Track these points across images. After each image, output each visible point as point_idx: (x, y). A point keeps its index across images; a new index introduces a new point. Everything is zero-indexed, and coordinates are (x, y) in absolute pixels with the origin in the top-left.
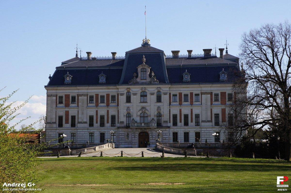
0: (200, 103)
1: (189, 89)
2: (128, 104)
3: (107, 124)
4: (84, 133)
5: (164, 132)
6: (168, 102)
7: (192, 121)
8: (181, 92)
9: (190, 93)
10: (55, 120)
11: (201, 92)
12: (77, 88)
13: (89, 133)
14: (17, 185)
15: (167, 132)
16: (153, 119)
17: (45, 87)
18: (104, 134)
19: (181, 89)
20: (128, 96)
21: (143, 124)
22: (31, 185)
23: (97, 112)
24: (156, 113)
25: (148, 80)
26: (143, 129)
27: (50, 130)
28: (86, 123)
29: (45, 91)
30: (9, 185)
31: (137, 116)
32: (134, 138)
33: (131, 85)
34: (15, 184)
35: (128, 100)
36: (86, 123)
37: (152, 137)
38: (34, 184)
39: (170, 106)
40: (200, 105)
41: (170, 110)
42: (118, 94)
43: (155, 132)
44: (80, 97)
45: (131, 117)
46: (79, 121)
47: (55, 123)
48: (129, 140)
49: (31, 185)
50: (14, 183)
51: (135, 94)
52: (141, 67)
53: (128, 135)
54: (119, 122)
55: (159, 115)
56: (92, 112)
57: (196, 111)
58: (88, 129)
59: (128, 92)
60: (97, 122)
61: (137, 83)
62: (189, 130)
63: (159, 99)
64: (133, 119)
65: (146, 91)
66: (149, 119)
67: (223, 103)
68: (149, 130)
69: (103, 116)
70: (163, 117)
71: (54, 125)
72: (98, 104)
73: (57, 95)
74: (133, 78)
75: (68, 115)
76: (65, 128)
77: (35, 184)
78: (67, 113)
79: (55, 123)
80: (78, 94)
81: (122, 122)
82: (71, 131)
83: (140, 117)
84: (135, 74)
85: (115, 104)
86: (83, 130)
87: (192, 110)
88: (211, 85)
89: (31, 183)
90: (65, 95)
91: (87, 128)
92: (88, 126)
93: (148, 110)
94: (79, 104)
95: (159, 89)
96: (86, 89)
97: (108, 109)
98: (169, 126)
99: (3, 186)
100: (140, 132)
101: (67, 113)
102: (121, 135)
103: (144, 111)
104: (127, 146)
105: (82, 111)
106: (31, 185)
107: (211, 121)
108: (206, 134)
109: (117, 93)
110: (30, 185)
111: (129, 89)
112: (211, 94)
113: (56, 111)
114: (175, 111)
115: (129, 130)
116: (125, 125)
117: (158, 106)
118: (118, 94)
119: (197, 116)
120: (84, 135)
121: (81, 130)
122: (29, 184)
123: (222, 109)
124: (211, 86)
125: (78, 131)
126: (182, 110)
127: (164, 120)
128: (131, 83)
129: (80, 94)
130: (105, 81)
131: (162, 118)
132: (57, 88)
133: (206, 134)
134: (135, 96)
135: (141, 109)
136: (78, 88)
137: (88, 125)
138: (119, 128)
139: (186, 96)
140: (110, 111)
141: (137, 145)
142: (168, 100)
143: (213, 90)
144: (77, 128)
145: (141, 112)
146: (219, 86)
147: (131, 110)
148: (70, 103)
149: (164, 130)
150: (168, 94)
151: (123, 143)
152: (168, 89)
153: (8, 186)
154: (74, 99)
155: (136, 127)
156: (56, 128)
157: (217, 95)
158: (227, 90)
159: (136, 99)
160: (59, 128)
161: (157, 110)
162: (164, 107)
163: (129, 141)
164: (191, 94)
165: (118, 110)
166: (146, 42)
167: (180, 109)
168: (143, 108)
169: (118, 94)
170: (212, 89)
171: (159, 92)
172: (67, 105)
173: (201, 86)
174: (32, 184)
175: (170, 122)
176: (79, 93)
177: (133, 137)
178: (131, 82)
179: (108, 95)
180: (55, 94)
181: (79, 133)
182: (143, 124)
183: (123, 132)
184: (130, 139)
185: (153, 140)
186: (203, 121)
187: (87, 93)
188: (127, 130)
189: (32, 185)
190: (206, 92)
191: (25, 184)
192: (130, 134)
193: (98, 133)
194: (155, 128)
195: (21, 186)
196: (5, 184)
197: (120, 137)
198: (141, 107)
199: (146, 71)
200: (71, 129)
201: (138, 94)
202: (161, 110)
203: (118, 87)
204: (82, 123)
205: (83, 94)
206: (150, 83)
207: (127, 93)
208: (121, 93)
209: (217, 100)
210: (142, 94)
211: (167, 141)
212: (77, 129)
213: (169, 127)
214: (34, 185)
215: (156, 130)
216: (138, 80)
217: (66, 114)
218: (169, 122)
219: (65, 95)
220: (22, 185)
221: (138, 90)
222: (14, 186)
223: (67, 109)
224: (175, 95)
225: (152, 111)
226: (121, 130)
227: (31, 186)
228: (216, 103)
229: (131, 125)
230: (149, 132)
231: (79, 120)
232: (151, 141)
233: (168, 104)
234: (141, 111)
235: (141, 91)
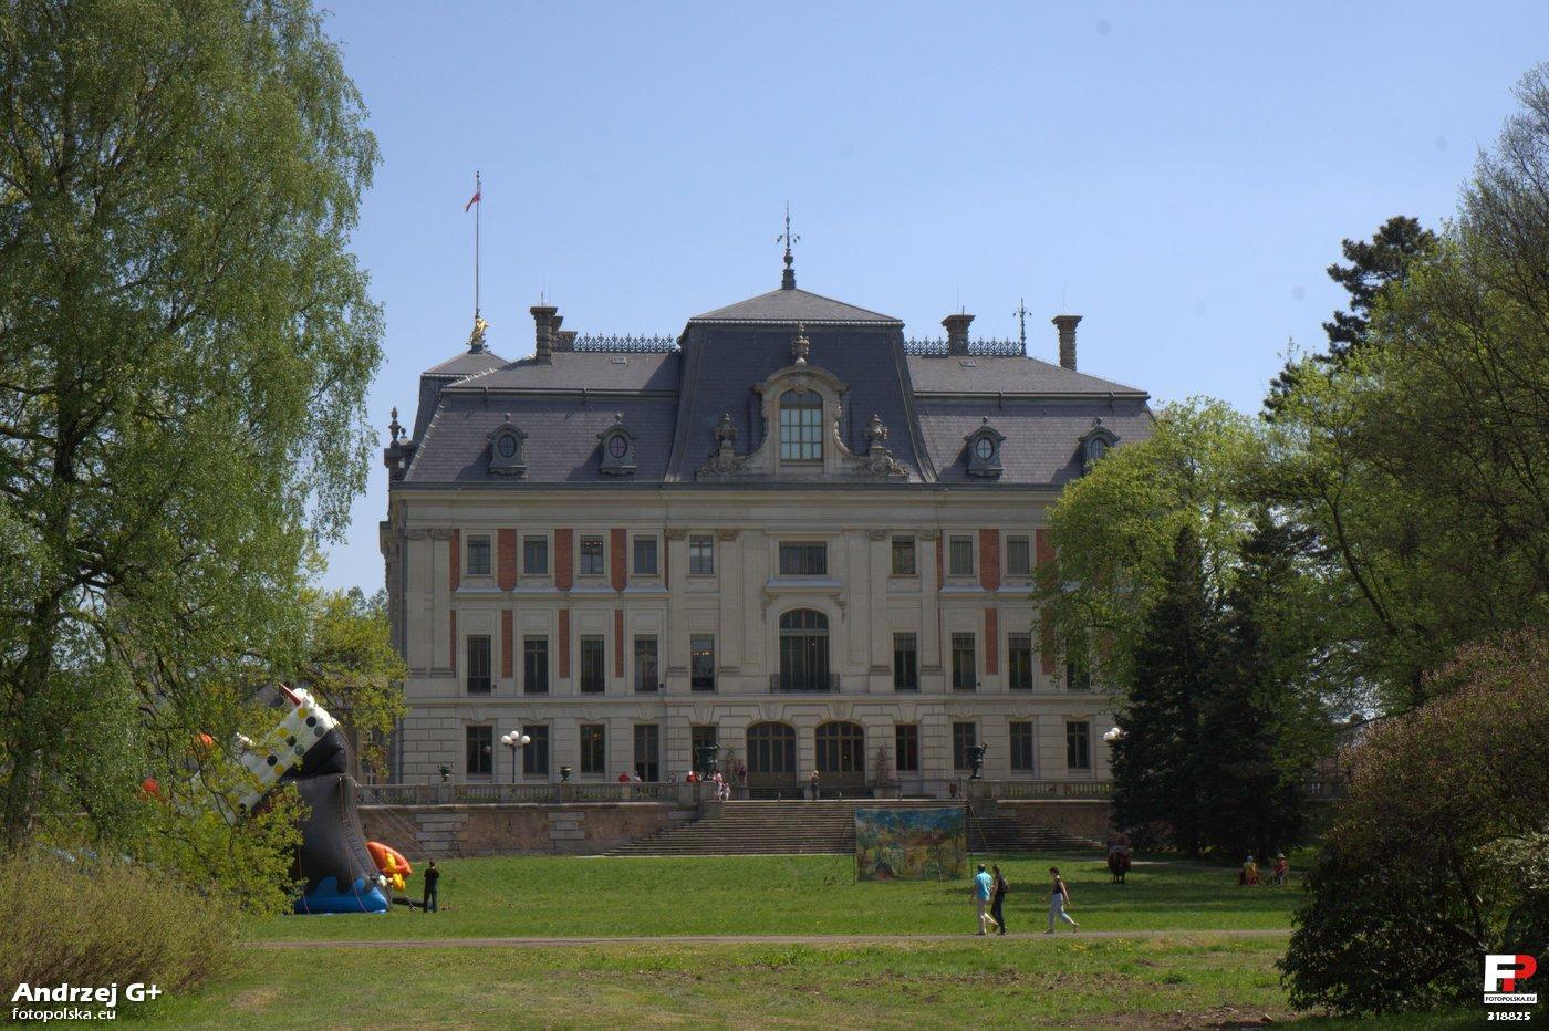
14: (78, 995)
22: (141, 994)
30: (42, 995)
34: (69, 992)
38: (154, 992)
49: (141, 994)
50: (65, 986)
69: (597, 642)
77: (159, 992)
89: (142, 986)
99: (15, 999)
106: (141, 994)
110: (138, 993)
122: (134, 994)
140: (629, 616)
153: (37, 999)
174: (148, 992)
189: (147, 997)
191: (114, 991)
195: (94, 999)
196: (23, 990)
214: (157, 995)
220: (98, 996)
222: (64, 998)
227: (141, 998)
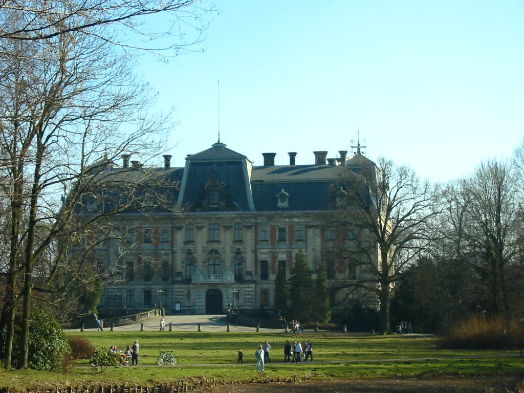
5: (247, 289)
13: (127, 291)
15: (251, 289)
18: (150, 292)
21: (212, 277)
32: (199, 298)
37: (228, 298)
81: (180, 274)
115: (191, 286)
149: (247, 286)
182: (212, 277)
183: (181, 290)
188: (187, 286)
192: (192, 292)
194: (232, 284)
226: (177, 286)
230: (223, 290)
233: (254, 245)
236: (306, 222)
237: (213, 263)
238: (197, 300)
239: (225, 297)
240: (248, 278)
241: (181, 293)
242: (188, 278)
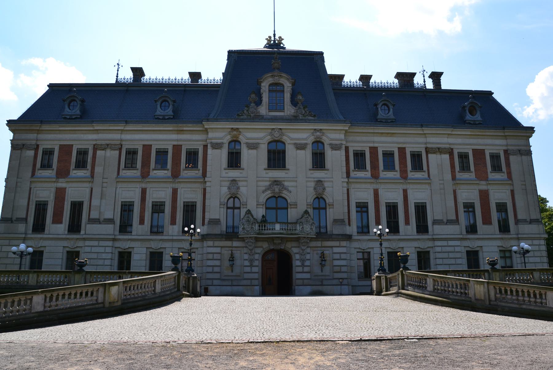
0: (426, 176)
1: (395, 139)
2: (234, 174)
3: (171, 227)
4: (102, 250)
5: (336, 250)
6: (344, 169)
7: (407, 222)
8: (376, 145)
9: (399, 148)
10: (25, 212)
11: (426, 148)
12: (93, 126)
15: (344, 250)
16: (306, 212)
17: (10, 123)
19: (376, 139)
20: (234, 151)
23: (144, 192)
24: (310, 200)
25: (289, 110)
26: (275, 241)
27: (8, 241)
28: (110, 221)
29: (10, 135)
31: (257, 205)
32: (251, 266)
33: (242, 120)
35: (234, 161)
36: (110, 221)
37: (303, 266)
39: (350, 180)
40: (426, 179)
41: (348, 190)
42: (207, 146)
43: (308, 250)
44: (99, 153)
45: (239, 208)
46: (91, 217)
47: (25, 220)
48: (234, 274)
51: (253, 146)
52: (270, 80)
53: (232, 259)
54: (206, 221)
55: (320, 203)
56: (132, 194)
57: (417, 195)
58: (114, 240)
59: (235, 141)
60: (142, 222)
61: (259, 118)
62: (401, 244)
63: (319, 161)
64: (249, 212)
65: (285, 139)
66: (293, 214)
67: (482, 176)
68: (294, 244)
70: (331, 210)
71: (21, 227)
72: (149, 172)
73: (38, 146)
74: (248, 106)
75: (63, 199)
76: (51, 236)
78: (60, 194)
79: (25, 220)
80: (94, 142)
81: (215, 222)
82: (65, 243)
83: (266, 208)
84: (253, 96)
85: (197, 172)
86: (102, 243)
87: (405, 192)
88: (448, 131)
90: (62, 147)
91: (113, 237)
92: (117, 232)
93: (290, 189)
94: (98, 170)
95: (318, 134)
96: (120, 132)
97: (176, 186)
98: (348, 233)
100: (266, 250)
101: (60, 194)
102: (210, 256)
103: (277, 190)
104: (229, 289)
105: (102, 190)
107: (456, 221)
108: (445, 255)
109: (204, 143)
111: (235, 133)
112: (451, 152)
113: (30, 188)
114: (363, 194)
115: (236, 244)
116: (225, 229)
117: (316, 180)
118: (205, 147)
119: (421, 209)
120: (104, 256)
121: (95, 243)
123: (481, 192)
124: (449, 134)
125: (88, 243)
126: (381, 192)
127: (336, 218)
128: (242, 117)
129: (101, 145)
130: (172, 114)
131: (330, 211)
132: (40, 126)
133: (445, 255)
134: (254, 152)
135: (270, 185)
136: (96, 128)
137: (118, 228)
138: (204, 237)
139: (388, 155)
141: (257, 289)
142: (344, 163)
143: (454, 144)
144: (84, 236)
145: (270, 195)
146: (469, 133)
147: (243, 190)
148: (73, 166)
150: (344, 148)
151: (215, 282)
152: (342, 136)
154: (83, 153)
155: (258, 234)
156: (26, 234)
157: (463, 157)
158: (486, 145)
159: (254, 160)
160: (33, 236)
161: (315, 189)
162: (332, 182)
163: (236, 276)
164: (402, 151)
165: (205, 190)
166: (274, 41)
167: (374, 190)
168: (276, 182)
169: (205, 147)
170: (451, 140)
171: (318, 142)
172: (63, 173)
173: (427, 131)
175: (349, 225)
176: (99, 142)
177: (247, 263)
178: (242, 115)
179: (177, 149)
180: (34, 142)
181: (88, 249)
183: (218, 250)
184: (237, 271)
185: (303, 272)
186: (435, 222)
187: (118, 142)
188: (228, 243)
190: (439, 148)
192: (237, 254)
193: (144, 250)
194: (312, 239)
197: (210, 263)
198: (269, 181)
199: (283, 91)
200: (68, 239)
201: (260, 145)
202: (324, 189)
203: (207, 125)
204: (100, 223)
205: (108, 145)
206: (294, 119)
207: (230, 143)
208: (214, 141)
209: (465, 168)
210: (273, 147)
211: (344, 275)
212: (84, 239)
213: (349, 238)
215: (313, 244)
216: (263, 110)
217: (56, 198)
218: (347, 221)
219: (62, 147)
221: (261, 135)
223: (62, 184)
224: (359, 156)
225: (300, 194)
226: (210, 243)
228: (465, 175)
229: (243, 228)
230: (295, 250)
231: (92, 212)
232: (299, 276)
233: (345, 176)
234: (269, 192)
235: (269, 137)
236: (426, 143)
237: (275, 206)
238: (248, 269)
239: (296, 263)
240: (337, 230)
241: (216, 256)
242: (230, 230)
